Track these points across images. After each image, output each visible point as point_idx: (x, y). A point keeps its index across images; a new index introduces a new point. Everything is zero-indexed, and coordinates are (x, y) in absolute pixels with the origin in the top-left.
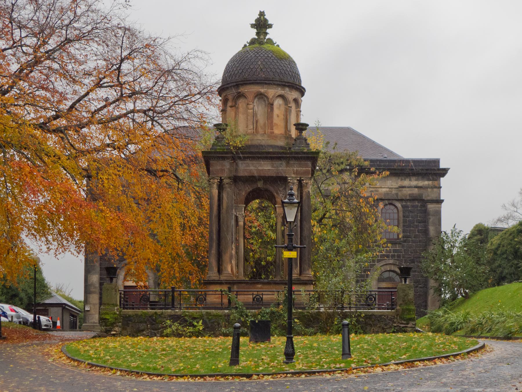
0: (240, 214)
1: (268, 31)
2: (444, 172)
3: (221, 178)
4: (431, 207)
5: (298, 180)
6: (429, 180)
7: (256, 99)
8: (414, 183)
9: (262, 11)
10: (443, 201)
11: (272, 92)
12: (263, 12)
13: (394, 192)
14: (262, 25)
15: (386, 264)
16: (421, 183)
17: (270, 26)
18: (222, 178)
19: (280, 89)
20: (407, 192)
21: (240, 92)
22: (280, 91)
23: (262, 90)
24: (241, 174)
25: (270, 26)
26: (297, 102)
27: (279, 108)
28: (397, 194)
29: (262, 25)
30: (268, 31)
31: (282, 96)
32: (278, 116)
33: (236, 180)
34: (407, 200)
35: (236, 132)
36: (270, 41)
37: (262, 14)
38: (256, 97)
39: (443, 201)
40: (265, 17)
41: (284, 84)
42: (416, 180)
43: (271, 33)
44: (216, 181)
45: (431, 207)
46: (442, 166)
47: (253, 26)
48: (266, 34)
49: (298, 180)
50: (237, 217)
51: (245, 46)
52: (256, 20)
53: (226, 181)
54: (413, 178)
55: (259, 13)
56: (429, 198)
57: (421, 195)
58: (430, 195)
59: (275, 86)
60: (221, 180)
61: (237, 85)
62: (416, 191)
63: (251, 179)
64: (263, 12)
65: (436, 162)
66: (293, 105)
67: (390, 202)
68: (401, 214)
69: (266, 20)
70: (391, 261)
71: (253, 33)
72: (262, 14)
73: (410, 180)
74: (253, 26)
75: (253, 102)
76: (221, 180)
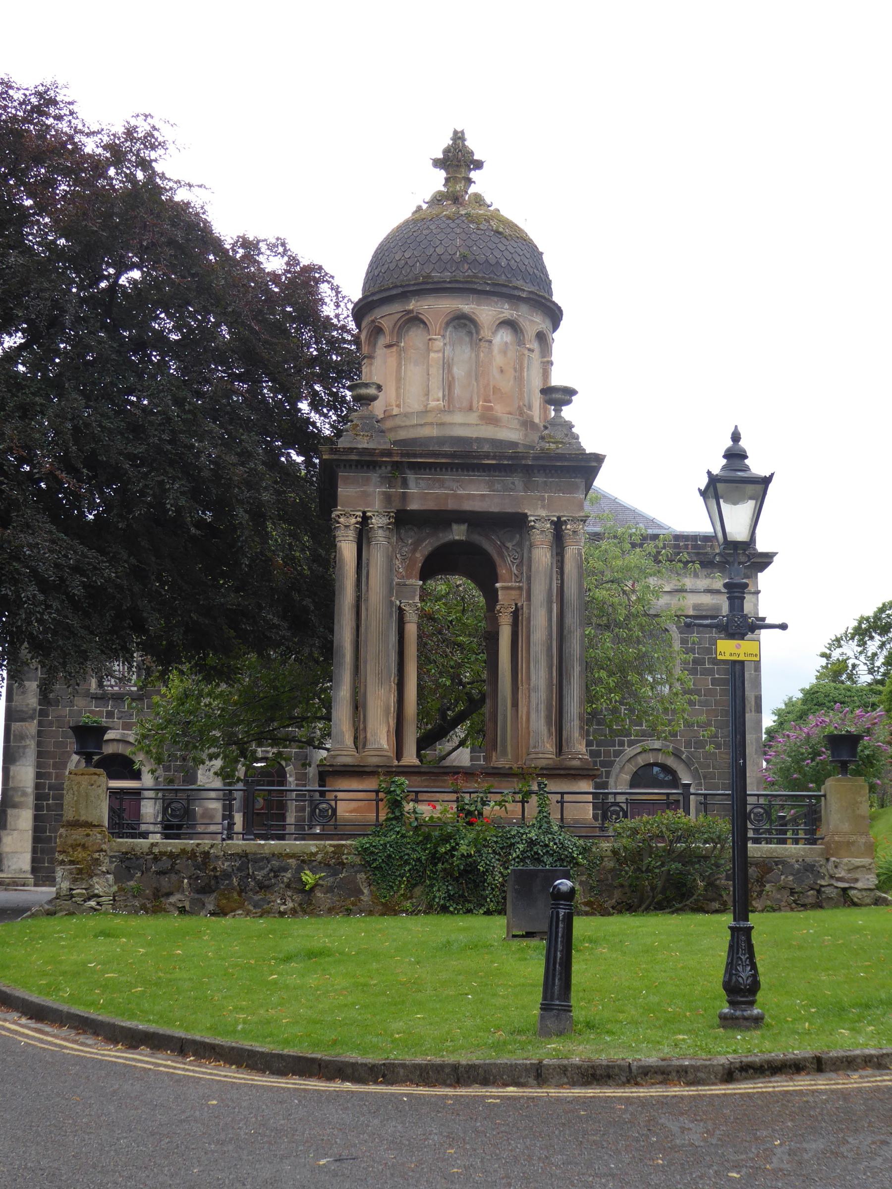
0: (409, 604)
1: (473, 175)
3: (364, 513)
5: (552, 522)
7: (450, 329)
9: (459, 130)
11: (487, 313)
12: (462, 132)
14: (457, 161)
17: (479, 165)
18: (369, 514)
19: (506, 306)
21: (411, 311)
22: (506, 311)
24: (414, 506)
25: (479, 165)
26: (543, 340)
27: (504, 352)
29: (457, 161)
30: (473, 175)
31: (511, 325)
32: (502, 371)
35: (398, 406)
36: (478, 199)
37: (458, 137)
38: (448, 324)
40: (466, 143)
41: (513, 297)
43: (481, 183)
44: (353, 520)
47: (437, 163)
48: (469, 181)
49: (552, 522)
51: (419, 208)
53: (377, 522)
55: (451, 135)
59: (495, 299)
60: (365, 519)
61: (405, 295)
63: (438, 519)
64: (462, 132)
71: (437, 180)
72: (458, 137)
74: (437, 163)
76: (365, 519)
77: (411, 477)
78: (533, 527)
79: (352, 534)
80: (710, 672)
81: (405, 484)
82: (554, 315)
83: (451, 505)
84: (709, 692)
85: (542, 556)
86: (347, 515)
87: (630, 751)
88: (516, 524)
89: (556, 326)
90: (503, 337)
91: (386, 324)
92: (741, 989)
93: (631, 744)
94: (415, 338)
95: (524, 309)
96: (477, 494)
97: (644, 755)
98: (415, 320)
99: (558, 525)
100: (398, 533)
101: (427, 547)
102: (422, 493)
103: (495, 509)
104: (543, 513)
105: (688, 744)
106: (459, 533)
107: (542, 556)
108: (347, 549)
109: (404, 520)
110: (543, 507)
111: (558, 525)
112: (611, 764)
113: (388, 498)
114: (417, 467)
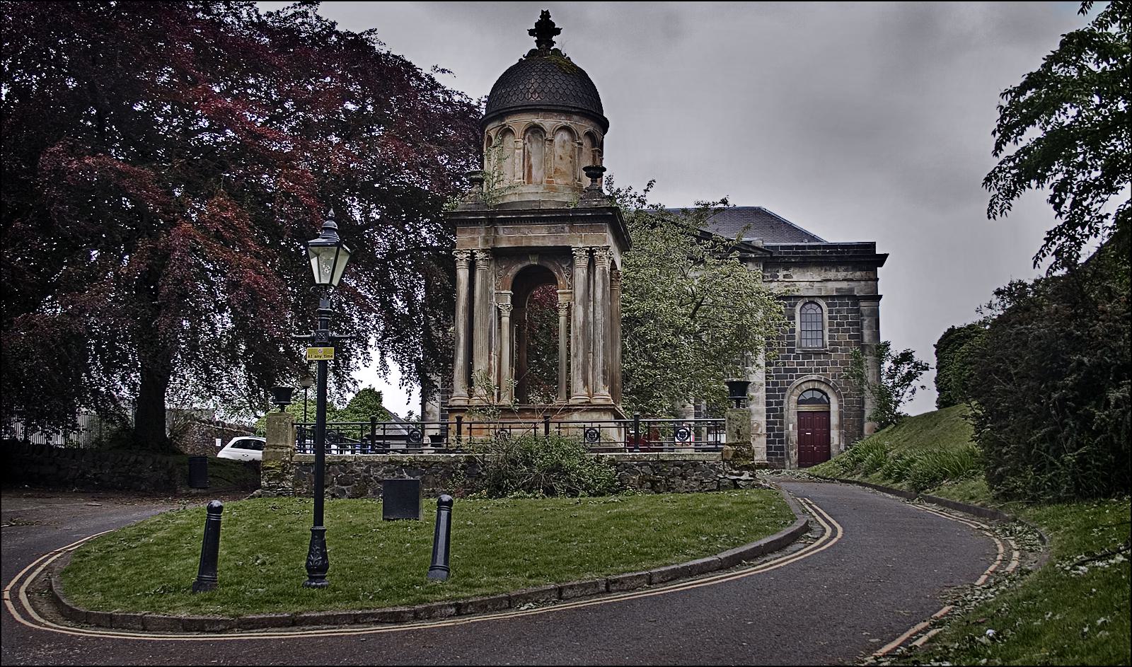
1: (554, 38)
8: (841, 275)
10: (881, 296)
15: (809, 381)
17: (558, 31)
22: (564, 121)
23: (537, 121)
30: (554, 38)
31: (567, 129)
33: (497, 255)
34: (833, 297)
38: (526, 131)
39: (881, 296)
44: (465, 256)
47: (531, 33)
53: (479, 256)
62: (844, 285)
66: (586, 142)
67: (811, 299)
68: (826, 315)
70: (814, 377)
73: (837, 271)
74: (531, 33)
75: (524, 139)
76: (473, 255)
77: (500, 227)
78: (575, 255)
79: (464, 263)
80: (848, 330)
81: (496, 231)
84: (847, 343)
85: (580, 273)
86: (460, 252)
91: (493, 134)
93: (798, 377)
94: (509, 139)
96: (540, 236)
97: (806, 384)
98: (507, 131)
99: (591, 252)
100: (496, 261)
101: (515, 269)
102: (507, 238)
103: (550, 244)
105: (834, 376)
107: (580, 273)
108: (463, 274)
110: (581, 242)
112: (785, 390)
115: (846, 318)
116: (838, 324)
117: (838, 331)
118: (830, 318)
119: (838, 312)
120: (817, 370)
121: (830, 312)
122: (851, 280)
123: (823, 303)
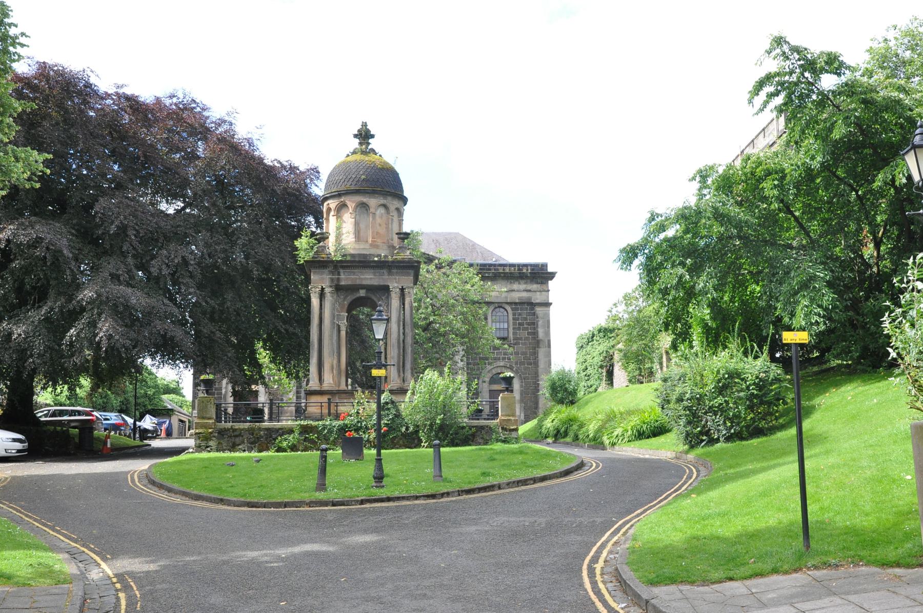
1: (370, 141)
2: (552, 276)
4: (539, 310)
6: (537, 283)
8: (523, 286)
13: (504, 295)
14: (364, 135)
16: (529, 287)
17: (373, 136)
20: (516, 297)
22: (382, 201)
24: (343, 283)
25: (373, 136)
26: (400, 213)
27: (381, 217)
28: (506, 297)
29: (364, 135)
34: (516, 303)
36: (373, 151)
37: (365, 125)
41: (385, 194)
42: (526, 283)
43: (374, 144)
45: (539, 310)
46: (550, 270)
47: (355, 136)
48: (369, 144)
50: (339, 326)
52: (359, 131)
54: (522, 282)
56: (538, 301)
57: (530, 298)
58: (538, 298)
60: (323, 289)
62: (525, 294)
63: (354, 288)
65: (544, 266)
66: (395, 214)
68: (511, 317)
69: (368, 131)
70: (502, 364)
72: (365, 125)
74: (355, 136)
76: (323, 289)
77: (341, 271)
79: (317, 295)
80: (527, 329)
81: (339, 274)
82: (404, 200)
83: (358, 282)
84: (526, 339)
85: (395, 302)
87: (489, 367)
88: (385, 290)
89: (405, 204)
90: (382, 211)
92: (379, 478)
95: (389, 198)
96: (369, 278)
99: (402, 289)
101: (350, 298)
102: (346, 278)
104: (396, 285)
105: (516, 363)
106: (362, 293)
107: (395, 302)
108: (315, 301)
109: (338, 289)
111: (402, 289)
113: (332, 280)
114: (343, 267)
115: (526, 319)
116: (519, 324)
117: (519, 329)
118: (514, 319)
119: (520, 314)
120: (504, 359)
121: (514, 314)
122: (530, 291)
123: (508, 308)
